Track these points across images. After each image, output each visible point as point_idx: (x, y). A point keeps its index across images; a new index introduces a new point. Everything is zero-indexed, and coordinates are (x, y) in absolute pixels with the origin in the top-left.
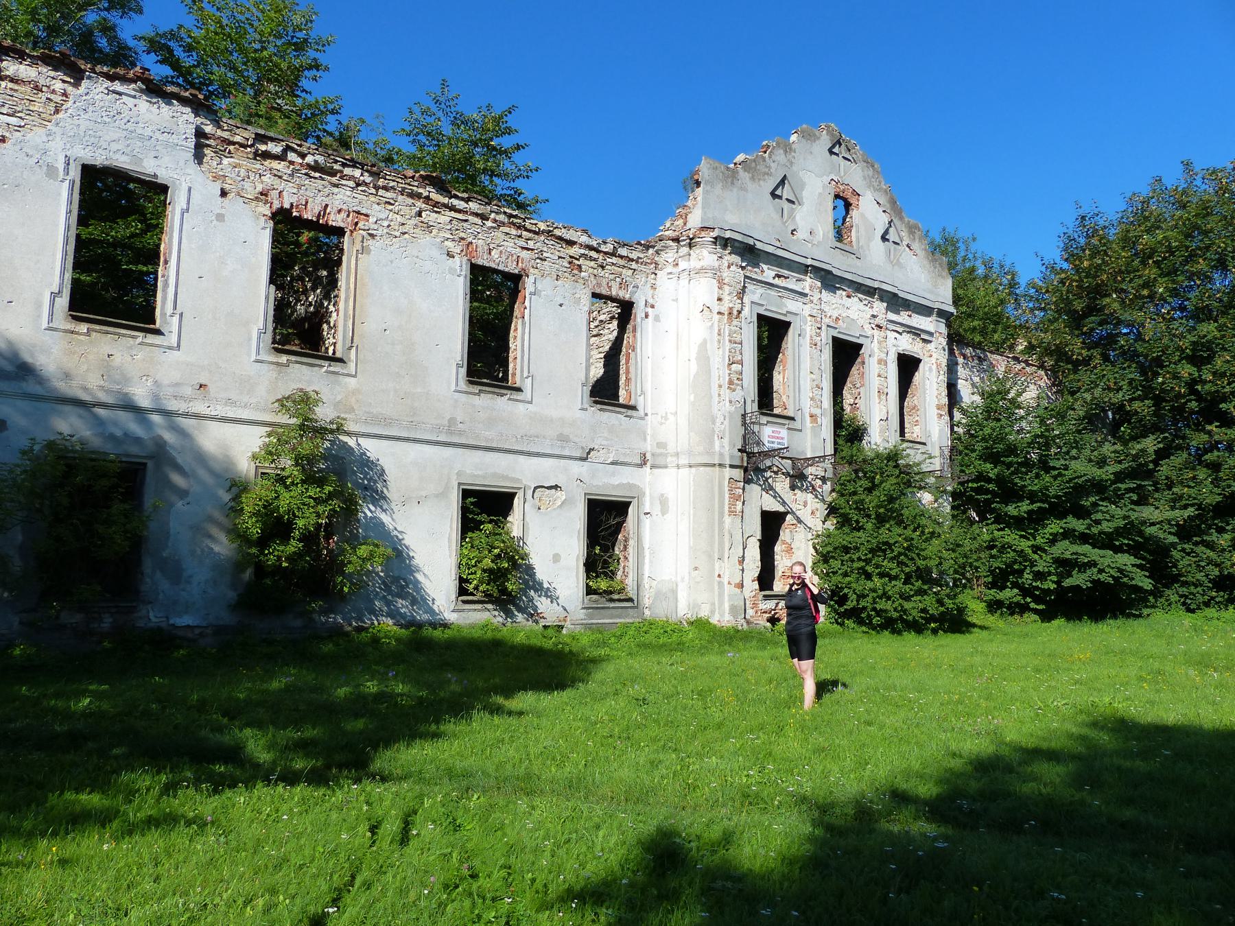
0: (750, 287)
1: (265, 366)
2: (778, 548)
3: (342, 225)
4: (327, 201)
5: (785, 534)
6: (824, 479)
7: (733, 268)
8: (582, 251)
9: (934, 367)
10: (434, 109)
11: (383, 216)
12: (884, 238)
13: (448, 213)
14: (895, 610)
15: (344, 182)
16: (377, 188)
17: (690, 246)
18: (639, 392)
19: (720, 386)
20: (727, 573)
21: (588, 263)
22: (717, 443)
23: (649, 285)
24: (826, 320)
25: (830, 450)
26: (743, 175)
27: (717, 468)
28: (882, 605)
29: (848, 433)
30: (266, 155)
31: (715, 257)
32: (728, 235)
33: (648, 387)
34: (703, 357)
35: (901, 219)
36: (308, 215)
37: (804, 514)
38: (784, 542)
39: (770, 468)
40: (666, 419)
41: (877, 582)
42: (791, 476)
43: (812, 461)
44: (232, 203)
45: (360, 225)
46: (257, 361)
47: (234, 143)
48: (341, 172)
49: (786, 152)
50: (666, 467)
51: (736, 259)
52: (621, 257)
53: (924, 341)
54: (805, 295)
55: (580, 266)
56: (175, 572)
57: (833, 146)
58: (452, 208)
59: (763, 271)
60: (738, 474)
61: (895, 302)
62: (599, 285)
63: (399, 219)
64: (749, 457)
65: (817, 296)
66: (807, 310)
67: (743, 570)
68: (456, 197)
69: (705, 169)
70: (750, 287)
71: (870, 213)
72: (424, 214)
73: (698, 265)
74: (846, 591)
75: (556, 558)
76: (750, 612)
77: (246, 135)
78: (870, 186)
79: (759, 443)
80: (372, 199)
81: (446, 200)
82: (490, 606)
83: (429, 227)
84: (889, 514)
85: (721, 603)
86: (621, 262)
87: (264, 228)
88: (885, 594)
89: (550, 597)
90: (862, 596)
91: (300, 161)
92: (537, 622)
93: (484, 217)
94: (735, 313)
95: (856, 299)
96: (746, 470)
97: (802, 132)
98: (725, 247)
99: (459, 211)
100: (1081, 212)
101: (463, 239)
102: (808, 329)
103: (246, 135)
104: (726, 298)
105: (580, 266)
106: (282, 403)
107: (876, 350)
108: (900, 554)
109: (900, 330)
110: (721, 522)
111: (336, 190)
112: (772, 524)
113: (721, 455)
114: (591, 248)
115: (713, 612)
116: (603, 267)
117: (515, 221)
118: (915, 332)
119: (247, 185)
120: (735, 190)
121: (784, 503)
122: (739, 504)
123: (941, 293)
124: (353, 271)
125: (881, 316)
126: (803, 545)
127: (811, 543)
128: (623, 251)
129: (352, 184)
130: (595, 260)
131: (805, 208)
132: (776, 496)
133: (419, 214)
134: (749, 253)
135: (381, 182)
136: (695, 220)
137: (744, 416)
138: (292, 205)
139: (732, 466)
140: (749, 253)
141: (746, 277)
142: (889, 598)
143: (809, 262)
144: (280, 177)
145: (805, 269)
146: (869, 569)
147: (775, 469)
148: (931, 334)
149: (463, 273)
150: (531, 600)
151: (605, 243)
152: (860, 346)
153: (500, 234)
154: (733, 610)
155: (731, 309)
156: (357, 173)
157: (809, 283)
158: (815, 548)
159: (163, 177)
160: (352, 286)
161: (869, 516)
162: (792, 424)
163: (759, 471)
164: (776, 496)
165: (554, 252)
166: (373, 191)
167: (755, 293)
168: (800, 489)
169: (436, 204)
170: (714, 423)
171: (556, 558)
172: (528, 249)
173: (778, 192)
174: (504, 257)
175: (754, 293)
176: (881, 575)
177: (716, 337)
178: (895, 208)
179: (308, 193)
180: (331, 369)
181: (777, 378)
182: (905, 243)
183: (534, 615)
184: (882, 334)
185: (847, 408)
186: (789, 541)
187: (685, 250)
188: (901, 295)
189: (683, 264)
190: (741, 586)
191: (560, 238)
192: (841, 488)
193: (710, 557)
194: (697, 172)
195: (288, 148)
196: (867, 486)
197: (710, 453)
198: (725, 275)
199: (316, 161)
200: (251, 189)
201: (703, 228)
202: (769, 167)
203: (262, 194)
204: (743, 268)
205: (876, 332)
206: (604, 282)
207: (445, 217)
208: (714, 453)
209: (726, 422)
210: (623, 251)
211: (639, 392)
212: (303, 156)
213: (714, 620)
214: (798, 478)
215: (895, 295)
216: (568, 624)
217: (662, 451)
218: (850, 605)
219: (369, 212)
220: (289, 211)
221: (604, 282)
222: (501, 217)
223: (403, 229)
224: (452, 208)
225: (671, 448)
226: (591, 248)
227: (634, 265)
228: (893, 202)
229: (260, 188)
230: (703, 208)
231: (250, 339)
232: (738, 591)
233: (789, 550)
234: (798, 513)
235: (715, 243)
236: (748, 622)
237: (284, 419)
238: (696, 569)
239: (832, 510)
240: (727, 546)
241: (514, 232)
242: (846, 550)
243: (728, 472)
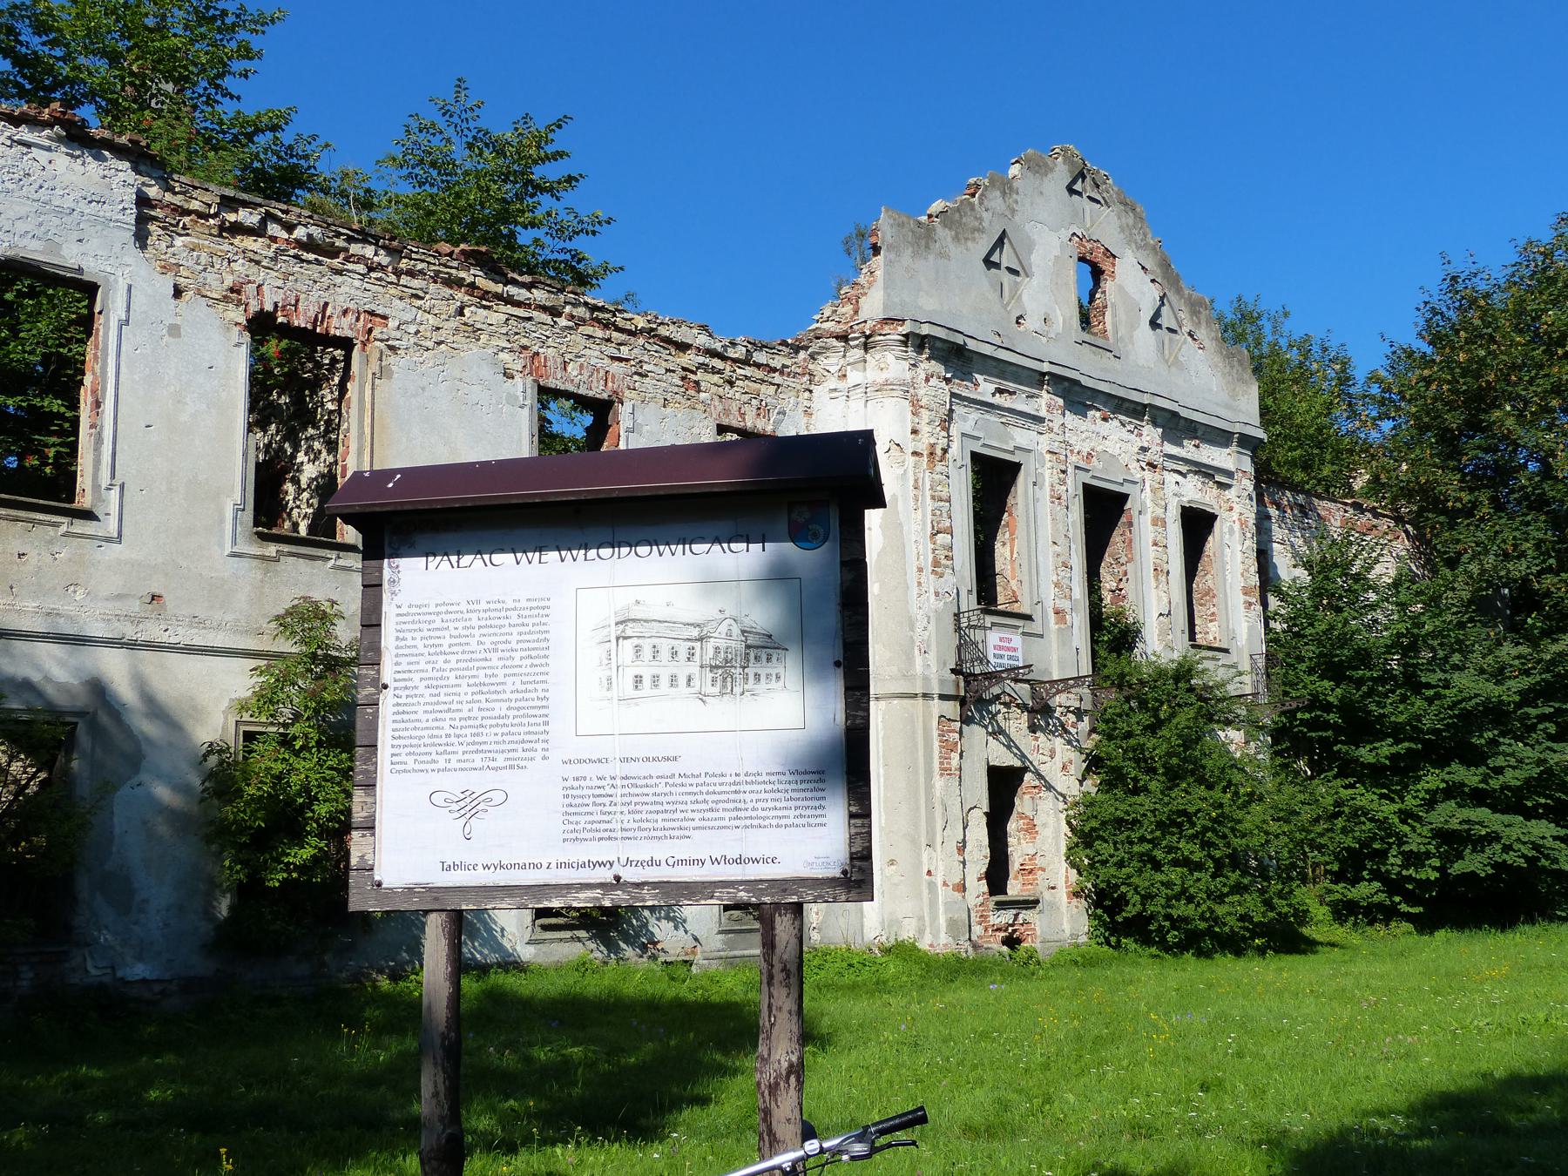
0: (959, 410)
1: (244, 563)
2: (1012, 826)
3: (350, 334)
4: (326, 296)
5: (1023, 803)
6: (1079, 714)
7: (933, 381)
8: (701, 359)
9: (1237, 527)
10: (441, 123)
11: (408, 317)
12: (1154, 324)
13: (502, 308)
14: (1202, 918)
15: (350, 266)
16: (398, 273)
17: (866, 347)
19: (920, 570)
20: (941, 868)
21: (709, 377)
22: (919, 660)
23: (801, 409)
24: (1073, 459)
25: (1086, 669)
26: (943, 234)
27: (920, 700)
28: (1182, 909)
29: (1112, 635)
30: (237, 229)
31: (906, 365)
32: (925, 330)
35: (1179, 291)
36: (300, 321)
37: (1051, 770)
38: (1022, 816)
39: (998, 697)
41: (1175, 874)
42: (1031, 711)
43: (1065, 684)
44: (193, 310)
45: (376, 333)
46: (234, 555)
47: (188, 213)
48: (347, 250)
49: (1004, 193)
51: (938, 368)
52: (758, 366)
53: (1221, 485)
54: (1040, 420)
55: (697, 383)
56: (122, 893)
57: (1074, 181)
58: (510, 301)
59: (977, 385)
60: (952, 709)
61: (1176, 426)
62: (727, 412)
63: (432, 320)
64: (967, 683)
65: (1058, 420)
66: (1044, 443)
67: (964, 863)
68: (514, 282)
69: (886, 227)
70: (959, 410)
71: (1132, 286)
72: (466, 311)
73: (881, 377)
74: (1124, 889)
76: (977, 930)
77: (207, 198)
78: (1130, 241)
79: (983, 660)
80: (393, 291)
81: (499, 288)
82: (582, 934)
83: (474, 332)
84: (1188, 765)
85: (934, 918)
86: (759, 374)
87: (238, 345)
88: (1184, 891)
89: (673, 919)
90: (1147, 898)
91: (286, 236)
92: (654, 958)
93: (554, 312)
94: (939, 452)
95: (1116, 423)
96: (963, 702)
97: (1028, 160)
98: (920, 349)
99: (518, 304)
100: (1452, 270)
101: (525, 348)
102: (1047, 473)
103: (207, 198)
104: (925, 429)
105: (697, 383)
106: (288, 621)
107: (1149, 503)
108: (1205, 829)
109: (1184, 469)
111: (338, 279)
112: (1004, 785)
113: (926, 679)
114: (713, 354)
115: (921, 931)
116: (731, 383)
117: (601, 316)
118: (1205, 472)
119: (211, 278)
120: (931, 258)
121: (1023, 756)
122: (955, 756)
123: (1241, 407)
124: (368, 406)
125: (1155, 448)
126: (1051, 821)
127: (1063, 816)
128: (760, 357)
129: (361, 268)
130: (720, 372)
131: (1035, 281)
132: (1010, 745)
133: (460, 312)
134: (956, 357)
135: (404, 264)
136: (873, 306)
137: (957, 616)
138: (276, 305)
139: (943, 697)
140: (956, 357)
141: (953, 395)
142: (1190, 899)
143: (1046, 367)
144: (258, 263)
145: (1038, 379)
146: (1159, 854)
148: (1230, 474)
149: (528, 402)
150: (645, 925)
151: (733, 344)
152: (1124, 497)
153: (579, 338)
154: (952, 925)
155: (933, 446)
156: (369, 251)
157: (1045, 402)
158: (1069, 823)
159: (92, 269)
160: (367, 430)
161: (1152, 771)
163: (983, 704)
164: (1010, 745)
165: (657, 362)
166: (393, 278)
167: (967, 420)
168: (1043, 731)
169: (485, 295)
170: (912, 628)
172: (620, 360)
173: (995, 258)
174: (586, 374)
175: (965, 420)
176: (1175, 863)
177: (911, 492)
178: (1168, 275)
179: (299, 286)
180: (341, 562)
181: (1001, 552)
182: (1185, 329)
183: (647, 945)
184: (1157, 477)
185: (1107, 598)
186: (1030, 814)
187: (859, 353)
188: (1184, 413)
189: (854, 376)
190: (962, 888)
191: (668, 340)
192: (1107, 725)
193: (914, 842)
194: (874, 233)
195: (269, 217)
196: (1144, 718)
197: (906, 676)
198: (921, 392)
199: (309, 236)
200: (218, 283)
201: (888, 321)
202: (981, 219)
203: (232, 290)
204: (948, 381)
205: (1148, 474)
206: (734, 407)
207: (498, 315)
208: (914, 676)
209: (932, 627)
210: (760, 357)
212: (290, 228)
213: (924, 945)
214: (1040, 714)
215: (1175, 414)
216: (698, 958)
218: (1131, 911)
219: (387, 312)
220: (272, 316)
221: (734, 407)
222: (581, 312)
223: (436, 337)
224: (510, 301)
226: (713, 354)
227: (777, 378)
228: (1165, 265)
229: (229, 281)
230: (885, 288)
231: (222, 521)
232: (958, 895)
233: (1031, 828)
234: (1043, 769)
235: (905, 344)
236: (975, 946)
237: (288, 646)
238: (892, 862)
239: (1094, 763)
240: (939, 825)
241: (599, 333)
242: (1119, 823)
243: (937, 707)
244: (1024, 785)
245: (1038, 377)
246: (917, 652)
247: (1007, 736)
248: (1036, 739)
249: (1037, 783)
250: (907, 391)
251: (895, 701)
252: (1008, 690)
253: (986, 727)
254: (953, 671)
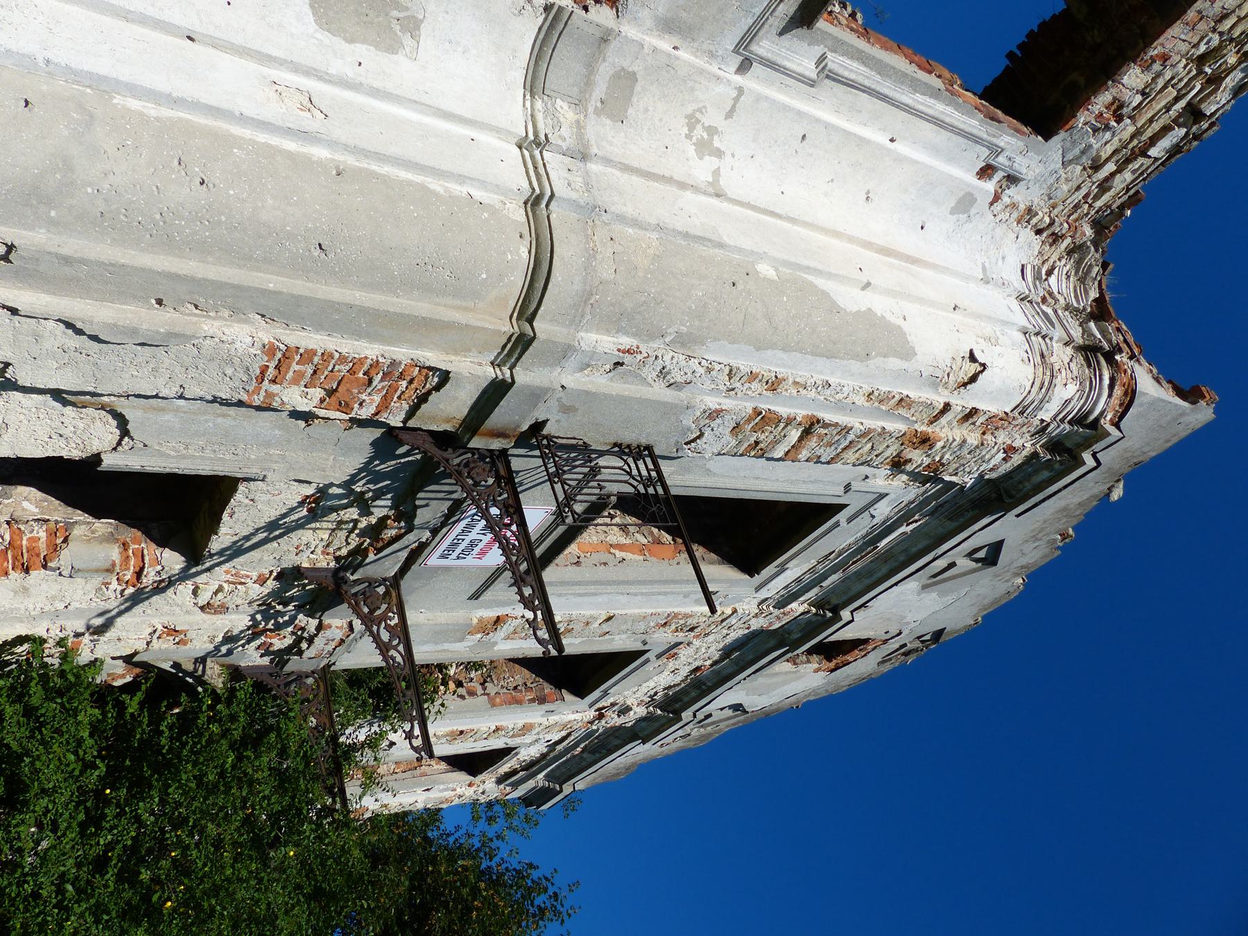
5: (95, 540)
18: (836, 62)
19: (774, 385)
27: (507, 327)
33: (825, 108)
37: (177, 607)
38: (60, 537)
40: (705, 148)
50: (534, 85)
60: (447, 409)
98: (1055, 446)
110: (238, 302)
112: (177, 511)
113: (563, 353)
121: (235, 551)
127: (40, 631)
132: (276, 529)
139: (496, 392)
147: (390, 533)
158: (20, 640)
170: (683, 342)
186: (66, 558)
209: (659, 391)
211: (836, 62)
217: (600, 90)
225: (605, 135)
234: (185, 589)
235: (1080, 420)
239: (161, 685)
243: (473, 370)
244: (151, 550)
245: (834, 601)
246: (627, 341)
247: (300, 525)
248: (262, 581)
249: (150, 577)
251: (522, 254)
252: (411, 537)
253: (348, 484)
254: (538, 427)
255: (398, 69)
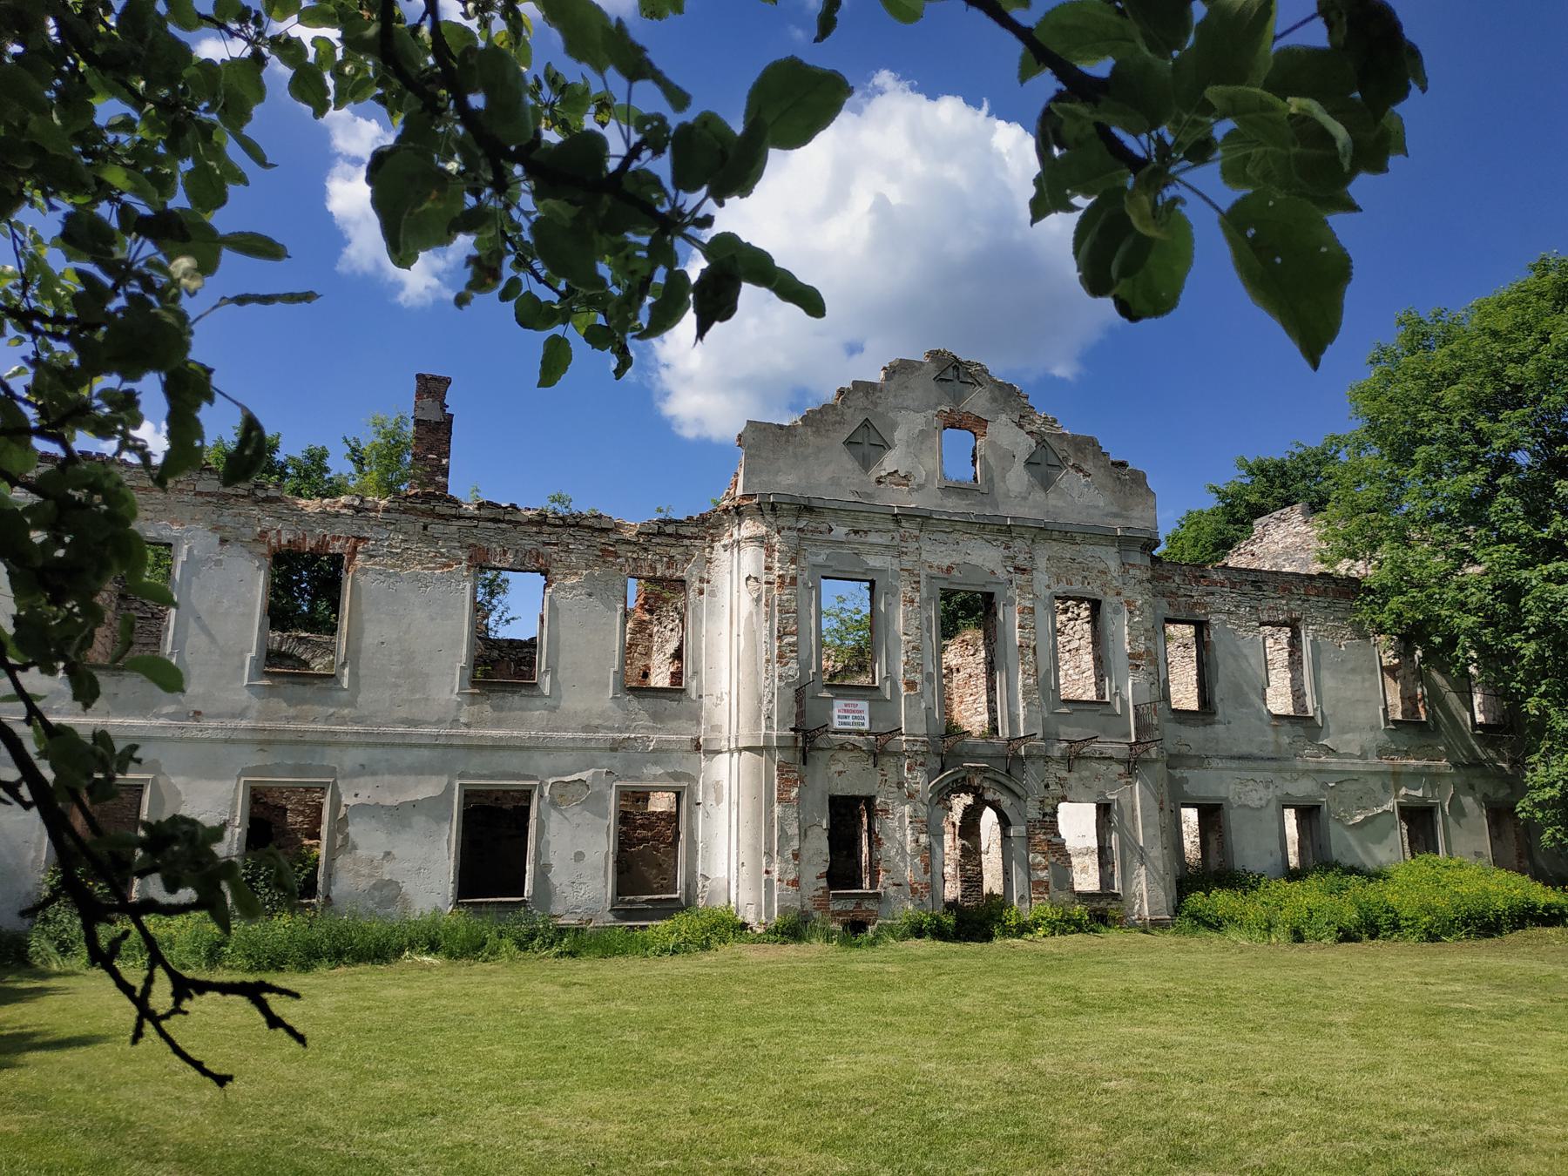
34: (752, 633)
50: (719, 752)
52: (670, 535)
75: (579, 856)
110: (769, 811)
113: (767, 737)
133: (425, 528)
162: (875, 695)
169: (441, 516)
171: (579, 856)
207: (454, 526)
250: (760, 540)
255: (726, 784)
